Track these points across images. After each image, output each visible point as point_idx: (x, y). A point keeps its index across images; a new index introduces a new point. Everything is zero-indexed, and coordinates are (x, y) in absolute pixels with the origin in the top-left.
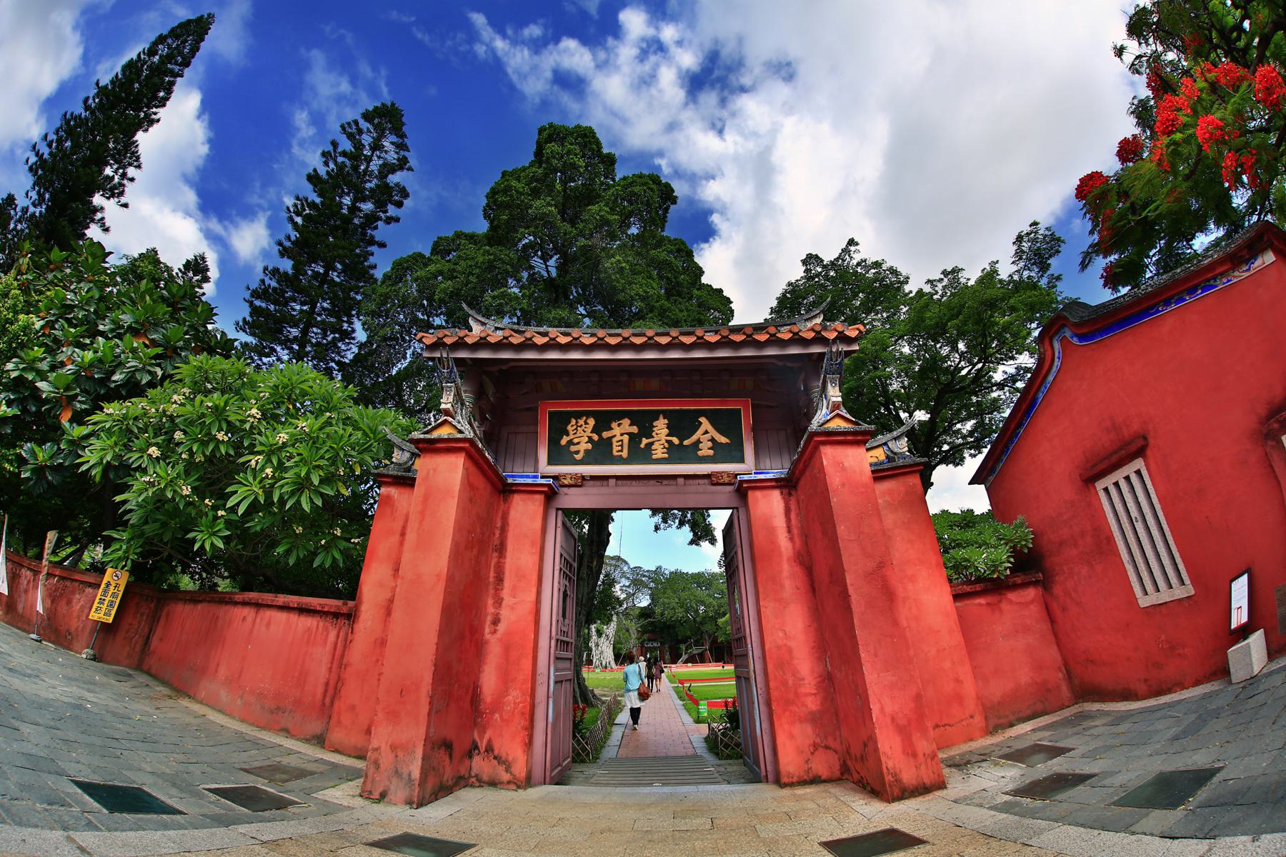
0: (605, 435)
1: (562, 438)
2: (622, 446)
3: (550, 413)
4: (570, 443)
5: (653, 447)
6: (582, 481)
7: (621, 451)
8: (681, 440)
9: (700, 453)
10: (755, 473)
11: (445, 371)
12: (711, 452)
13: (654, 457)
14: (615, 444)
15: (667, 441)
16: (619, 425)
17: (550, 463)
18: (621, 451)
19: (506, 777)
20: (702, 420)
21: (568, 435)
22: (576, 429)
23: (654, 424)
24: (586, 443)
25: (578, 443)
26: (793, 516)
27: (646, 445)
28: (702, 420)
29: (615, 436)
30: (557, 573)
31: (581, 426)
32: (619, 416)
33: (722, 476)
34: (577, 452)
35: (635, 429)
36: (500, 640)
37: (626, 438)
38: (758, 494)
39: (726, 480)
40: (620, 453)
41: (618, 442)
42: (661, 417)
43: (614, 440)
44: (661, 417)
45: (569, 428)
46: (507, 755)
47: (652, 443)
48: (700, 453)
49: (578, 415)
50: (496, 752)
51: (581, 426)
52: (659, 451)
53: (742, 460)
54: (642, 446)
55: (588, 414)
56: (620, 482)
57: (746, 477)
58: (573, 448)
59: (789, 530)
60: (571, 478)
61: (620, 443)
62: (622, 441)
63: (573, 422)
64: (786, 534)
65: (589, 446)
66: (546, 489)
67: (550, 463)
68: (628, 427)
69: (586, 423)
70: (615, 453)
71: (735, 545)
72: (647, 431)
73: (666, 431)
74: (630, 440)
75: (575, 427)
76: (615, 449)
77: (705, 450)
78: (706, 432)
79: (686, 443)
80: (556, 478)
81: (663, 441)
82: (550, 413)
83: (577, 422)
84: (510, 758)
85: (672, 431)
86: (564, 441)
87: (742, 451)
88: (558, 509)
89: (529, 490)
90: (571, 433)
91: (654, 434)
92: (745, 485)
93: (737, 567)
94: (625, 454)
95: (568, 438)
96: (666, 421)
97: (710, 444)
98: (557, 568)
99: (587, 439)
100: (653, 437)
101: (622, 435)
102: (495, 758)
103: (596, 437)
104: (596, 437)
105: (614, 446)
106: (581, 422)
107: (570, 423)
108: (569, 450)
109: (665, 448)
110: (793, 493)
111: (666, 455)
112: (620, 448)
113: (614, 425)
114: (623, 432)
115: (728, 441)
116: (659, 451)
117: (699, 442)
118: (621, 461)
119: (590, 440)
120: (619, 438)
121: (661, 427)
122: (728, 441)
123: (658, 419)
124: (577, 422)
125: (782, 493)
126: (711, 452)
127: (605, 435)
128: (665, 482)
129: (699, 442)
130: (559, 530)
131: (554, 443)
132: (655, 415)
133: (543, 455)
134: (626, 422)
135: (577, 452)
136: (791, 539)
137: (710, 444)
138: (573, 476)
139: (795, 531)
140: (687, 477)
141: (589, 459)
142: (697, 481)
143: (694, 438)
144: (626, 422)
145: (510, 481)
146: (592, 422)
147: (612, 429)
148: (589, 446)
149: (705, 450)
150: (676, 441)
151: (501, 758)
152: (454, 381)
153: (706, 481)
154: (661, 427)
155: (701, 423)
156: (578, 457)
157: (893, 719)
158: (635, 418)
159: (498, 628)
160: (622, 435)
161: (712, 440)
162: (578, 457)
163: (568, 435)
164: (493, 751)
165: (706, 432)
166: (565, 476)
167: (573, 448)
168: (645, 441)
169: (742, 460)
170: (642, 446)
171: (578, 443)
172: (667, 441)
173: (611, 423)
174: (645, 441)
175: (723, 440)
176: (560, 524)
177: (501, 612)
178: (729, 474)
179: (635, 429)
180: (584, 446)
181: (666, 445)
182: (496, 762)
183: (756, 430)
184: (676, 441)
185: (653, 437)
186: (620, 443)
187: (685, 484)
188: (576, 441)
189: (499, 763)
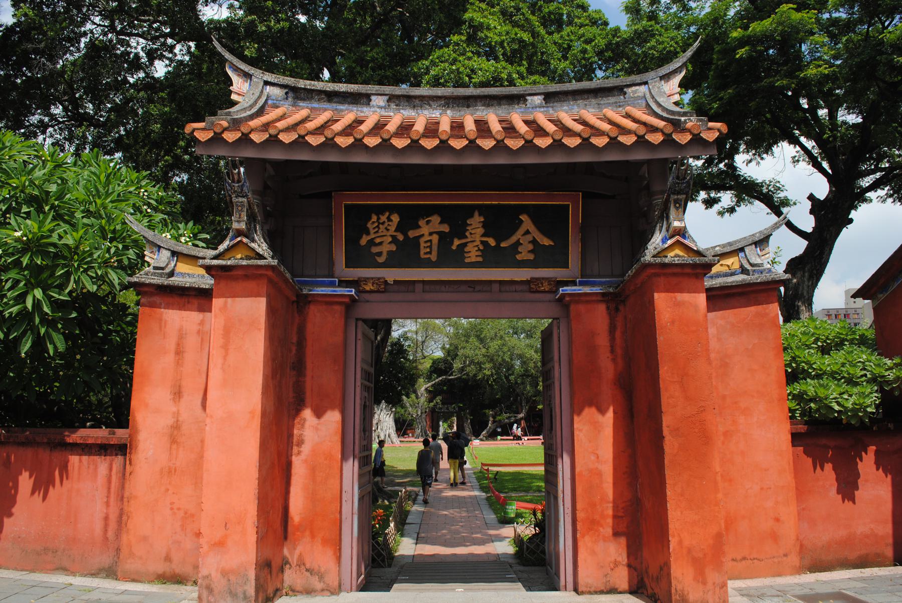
0: (412, 234)
1: (361, 237)
2: (430, 247)
3: (346, 206)
4: (371, 243)
5: (466, 249)
6: (384, 287)
7: (430, 253)
8: (498, 242)
9: (518, 257)
10: (582, 284)
11: (237, 185)
12: (531, 257)
13: (467, 260)
14: (422, 245)
15: (482, 242)
16: (428, 222)
17: (347, 266)
18: (430, 253)
19: (319, 586)
20: (524, 217)
21: (368, 233)
22: (378, 227)
23: (468, 222)
24: (390, 243)
25: (381, 243)
26: (618, 334)
27: (458, 246)
28: (524, 217)
29: (423, 235)
30: (358, 390)
31: (383, 223)
32: (428, 211)
33: (542, 284)
34: (380, 254)
35: (445, 228)
36: (306, 461)
37: (435, 238)
38: (582, 308)
39: (546, 287)
40: (428, 256)
41: (426, 242)
42: (476, 214)
43: (422, 240)
44: (476, 214)
45: (369, 225)
46: (319, 566)
47: (465, 245)
48: (518, 257)
49: (380, 210)
50: (308, 566)
51: (383, 223)
52: (473, 254)
53: (566, 265)
54: (454, 247)
55: (392, 209)
56: (427, 287)
57: (569, 289)
58: (375, 250)
59: (612, 351)
60: (373, 284)
61: (429, 244)
62: (430, 241)
63: (374, 218)
64: (609, 354)
65: (393, 248)
66: (347, 300)
67: (347, 266)
68: (437, 226)
69: (389, 219)
70: (423, 256)
71: (552, 358)
72: (459, 230)
73: (481, 231)
74: (439, 241)
75: (376, 224)
76: (422, 251)
77: (524, 254)
78: (527, 232)
79: (503, 245)
80: (354, 283)
81: (478, 243)
82: (346, 206)
83: (379, 219)
84: (323, 570)
85: (489, 229)
86: (364, 241)
87: (567, 255)
88: (357, 319)
89: (329, 301)
90: (372, 231)
91: (467, 234)
92: (567, 299)
93: (554, 383)
94: (434, 257)
95: (369, 238)
96: (482, 219)
97: (531, 247)
98: (358, 384)
99: (390, 239)
100: (466, 237)
101: (431, 234)
102: (307, 570)
103: (401, 237)
104: (401, 237)
105: (422, 247)
106: (383, 218)
107: (370, 218)
108: (370, 251)
109: (479, 250)
110: (621, 307)
111: (480, 259)
112: (428, 250)
113: (422, 223)
114: (432, 230)
115: (552, 243)
116: (473, 254)
117: (518, 243)
118: (428, 264)
119: (394, 240)
120: (427, 238)
121: (476, 225)
122: (552, 243)
123: (471, 216)
124: (379, 219)
125: (608, 308)
126: (531, 257)
127: (412, 234)
128: (478, 288)
129: (518, 243)
130: (359, 343)
131: (352, 241)
132: (469, 211)
133: (340, 257)
134: (436, 219)
135: (380, 254)
136: (614, 360)
137: (531, 247)
138: (376, 280)
139: (619, 351)
140: (501, 282)
141: (393, 262)
142: (513, 288)
143: (513, 239)
144: (436, 219)
145: (305, 292)
146: (396, 218)
147: (419, 227)
148: (393, 248)
149: (524, 254)
150: (492, 242)
151: (313, 570)
152: (246, 196)
153: (525, 287)
154: (476, 225)
155: (521, 221)
156: (381, 260)
157: (689, 551)
158: (447, 214)
159: (301, 449)
160: (431, 234)
161: (534, 242)
162: (381, 260)
163: (368, 233)
164: (304, 564)
165: (527, 232)
166: (366, 280)
167: (375, 250)
168: (457, 242)
169: (566, 265)
170: (454, 247)
171: (381, 243)
172: (482, 242)
173: (418, 220)
174: (457, 242)
175: (546, 242)
176: (360, 336)
177: (305, 433)
178: (548, 280)
179: (445, 228)
180: (387, 247)
181: (481, 247)
182: (308, 574)
183: (584, 229)
184: (492, 242)
185: (466, 237)
186: (429, 244)
187: (500, 291)
188: (378, 241)
189: (311, 574)
